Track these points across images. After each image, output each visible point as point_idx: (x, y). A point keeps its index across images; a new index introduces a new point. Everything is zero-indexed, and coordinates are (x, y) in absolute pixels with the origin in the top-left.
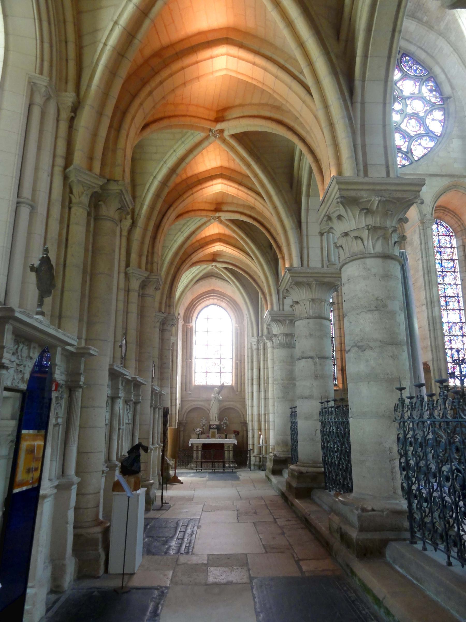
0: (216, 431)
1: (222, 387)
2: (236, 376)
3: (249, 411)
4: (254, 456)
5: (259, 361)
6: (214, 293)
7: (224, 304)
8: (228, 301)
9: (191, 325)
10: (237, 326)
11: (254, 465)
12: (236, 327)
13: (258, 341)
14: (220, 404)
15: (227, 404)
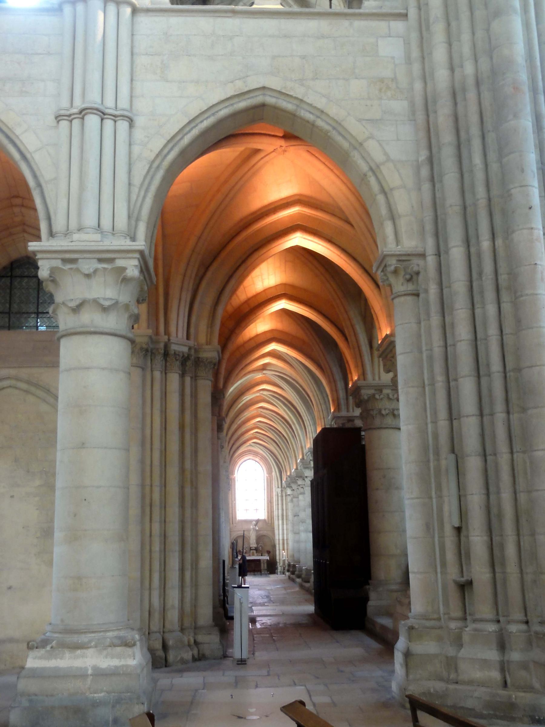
0: (255, 551)
1: (258, 521)
2: (268, 512)
3: (277, 537)
4: (280, 566)
5: (282, 504)
6: (250, 452)
7: (257, 459)
8: (261, 458)
9: (234, 476)
10: (268, 476)
11: (280, 572)
12: (267, 476)
13: (282, 491)
14: (256, 533)
15: (261, 533)
